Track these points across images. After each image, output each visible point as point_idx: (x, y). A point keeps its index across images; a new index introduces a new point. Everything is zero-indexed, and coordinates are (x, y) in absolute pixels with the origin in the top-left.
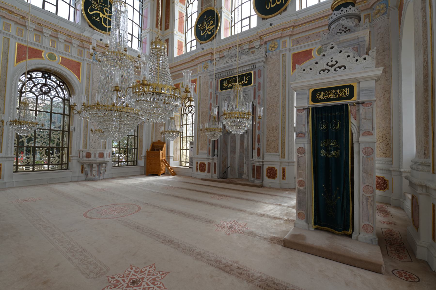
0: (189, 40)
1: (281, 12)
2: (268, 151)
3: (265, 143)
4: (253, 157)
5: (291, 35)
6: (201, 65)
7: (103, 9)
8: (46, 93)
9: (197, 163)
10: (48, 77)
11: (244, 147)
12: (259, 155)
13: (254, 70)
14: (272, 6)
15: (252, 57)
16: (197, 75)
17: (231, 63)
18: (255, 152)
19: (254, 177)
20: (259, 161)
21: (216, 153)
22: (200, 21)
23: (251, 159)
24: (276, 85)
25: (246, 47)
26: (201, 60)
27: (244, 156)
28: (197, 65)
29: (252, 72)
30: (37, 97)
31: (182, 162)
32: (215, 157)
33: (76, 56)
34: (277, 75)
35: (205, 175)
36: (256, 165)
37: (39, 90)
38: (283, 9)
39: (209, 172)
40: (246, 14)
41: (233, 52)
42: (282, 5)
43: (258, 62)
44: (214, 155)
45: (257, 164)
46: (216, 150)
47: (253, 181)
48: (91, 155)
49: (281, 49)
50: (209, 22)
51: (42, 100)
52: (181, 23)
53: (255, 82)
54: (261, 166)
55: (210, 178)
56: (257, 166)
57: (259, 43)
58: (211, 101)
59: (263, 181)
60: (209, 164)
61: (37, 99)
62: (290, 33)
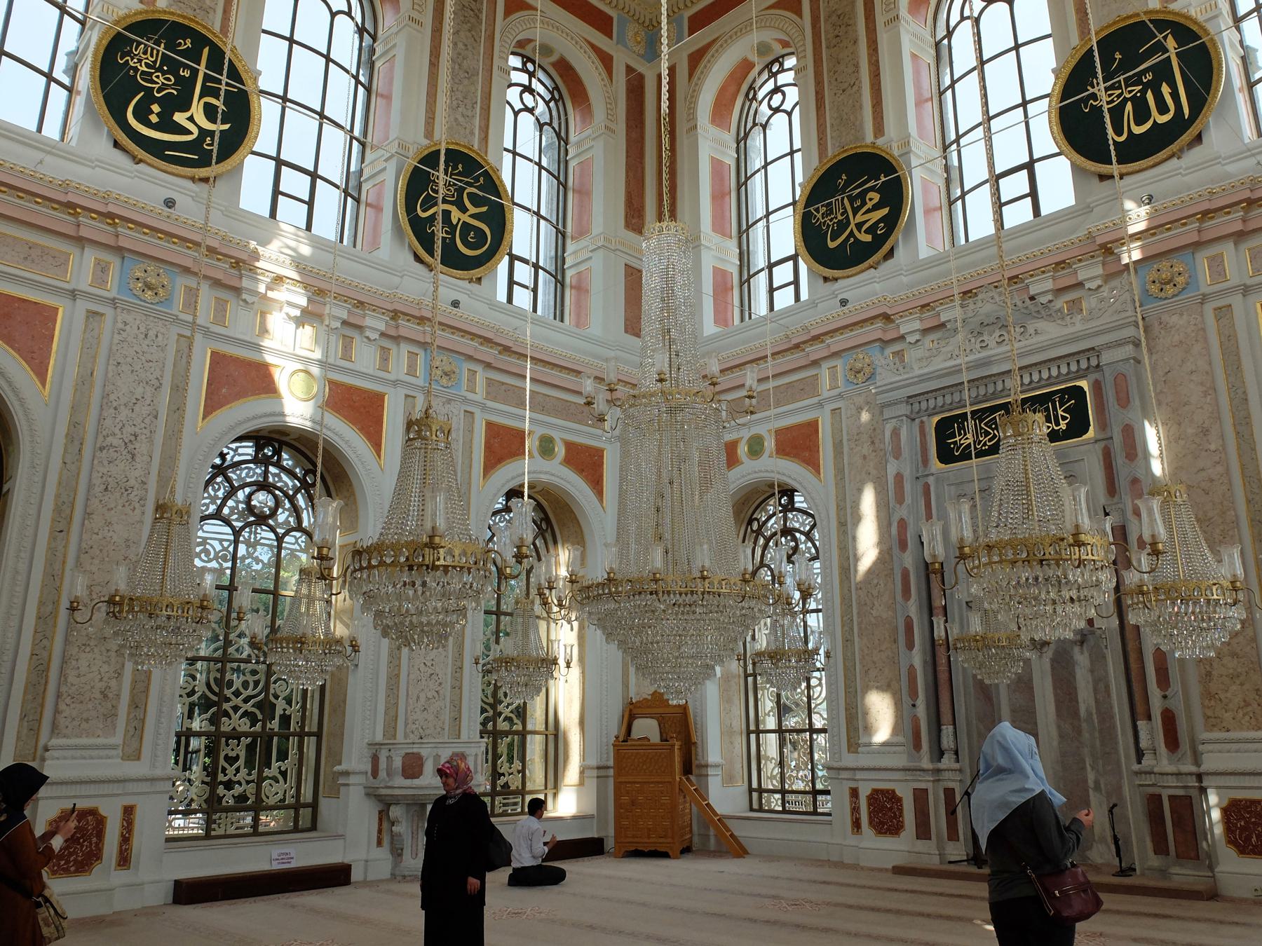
0: (760, 261)
1: (1181, 150)
2: (1213, 722)
3: (1195, 691)
4: (1140, 755)
5: (1239, 236)
6: (838, 363)
7: (460, 191)
8: (262, 519)
9: (854, 793)
10: (272, 456)
11: (1076, 714)
12: (1172, 742)
13: (1093, 376)
14: (1138, 130)
15: (1077, 325)
16: (820, 405)
17: (984, 354)
18: (1152, 733)
19: (1160, 847)
20: (1179, 774)
21: (947, 741)
22: (821, 191)
23: (1136, 767)
24: (1205, 432)
25: (1043, 285)
26: (837, 342)
27: (1086, 751)
28: (815, 363)
29: (1084, 384)
30: (237, 533)
31: (761, 791)
32: (947, 762)
33: (371, 371)
34: (1206, 394)
35: (901, 847)
36: (1165, 794)
37: (241, 506)
38: (1186, 137)
39: (923, 832)
40: (1010, 152)
41: (985, 307)
42: (1179, 126)
43: (1109, 346)
44: (941, 754)
45: (1170, 789)
46: (947, 730)
47: (1163, 873)
48: (422, 766)
49: (1204, 289)
50: (862, 196)
51: (248, 544)
52: (719, 197)
53: (1103, 425)
54: (1194, 793)
55: (934, 862)
56: (1171, 798)
57: (1099, 270)
58: (903, 512)
59: (1211, 868)
60: (920, 797)
61: (236, 542)
62: (1238, 226)
